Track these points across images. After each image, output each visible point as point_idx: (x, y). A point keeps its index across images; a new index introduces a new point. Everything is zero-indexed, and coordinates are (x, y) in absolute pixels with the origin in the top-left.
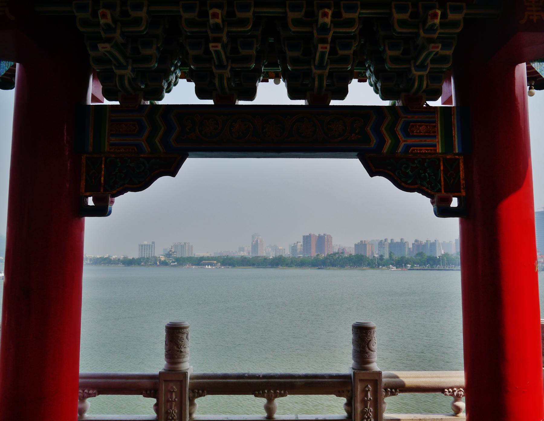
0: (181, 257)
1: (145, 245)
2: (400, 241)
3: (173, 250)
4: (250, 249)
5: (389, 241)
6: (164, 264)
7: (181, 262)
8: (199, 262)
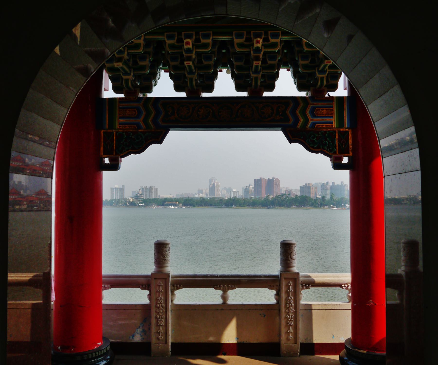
0: (148, 199)
1: (116, 188)
2: (340, 184)
3: (141, 193)
4: (208, 191)
5: (331, 184)
6: (133, 204)
7: (148, 203)
8: (164, 203)
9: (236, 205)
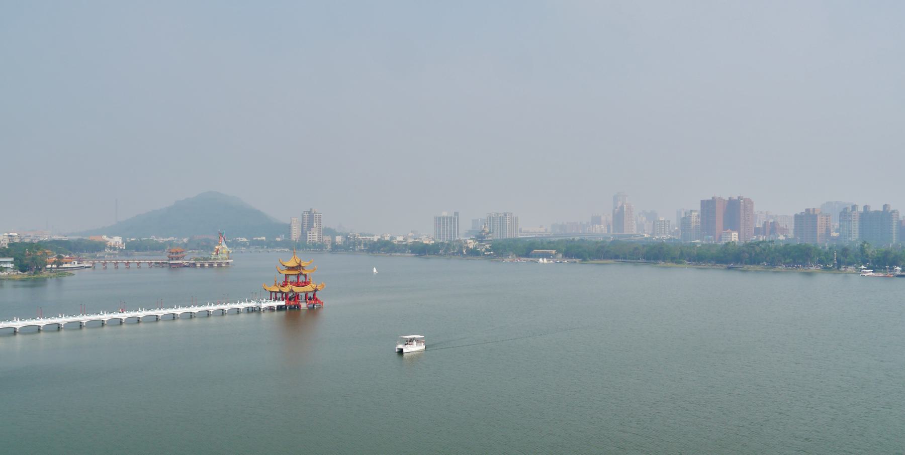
1: (444, 218)
2: (882, 209)
3: (487, 230)
4: (610, 219)
5: (861, 209)
8: (528, 249)
9: (664, 260)
